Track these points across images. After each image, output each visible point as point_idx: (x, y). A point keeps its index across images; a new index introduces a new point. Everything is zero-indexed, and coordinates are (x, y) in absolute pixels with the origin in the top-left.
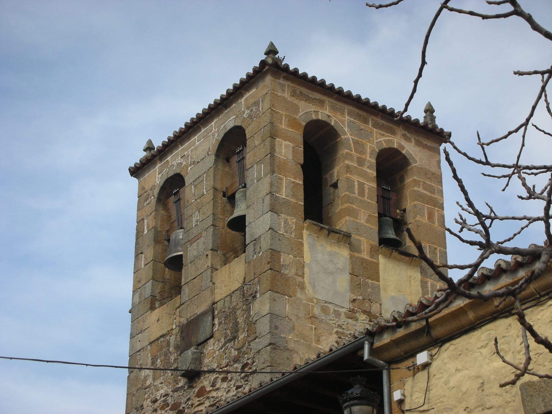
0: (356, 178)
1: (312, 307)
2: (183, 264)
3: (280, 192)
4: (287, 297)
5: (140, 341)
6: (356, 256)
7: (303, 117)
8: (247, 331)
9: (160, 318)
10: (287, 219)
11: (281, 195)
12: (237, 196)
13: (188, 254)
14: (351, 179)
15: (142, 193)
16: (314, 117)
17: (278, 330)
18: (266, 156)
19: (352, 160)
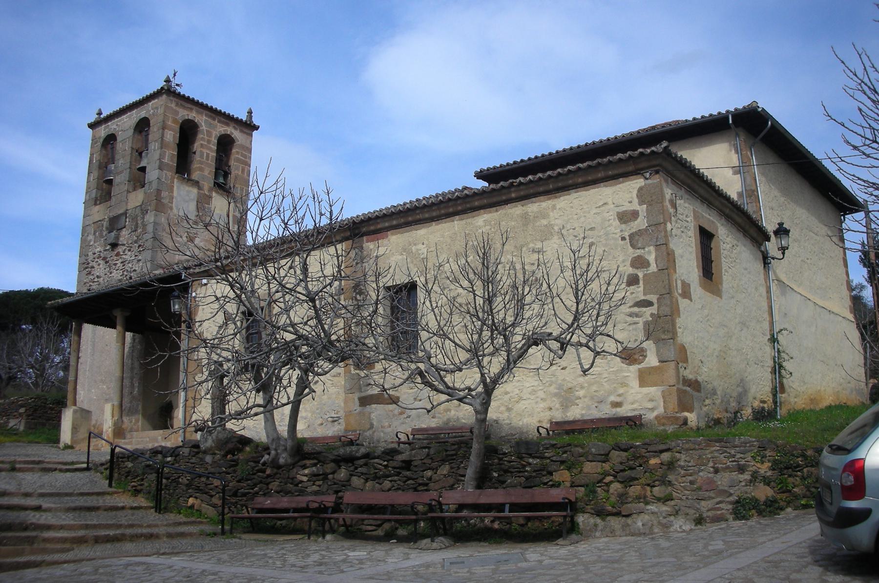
0: (205, 151)
12: (143, 154)
16: (187, 118)
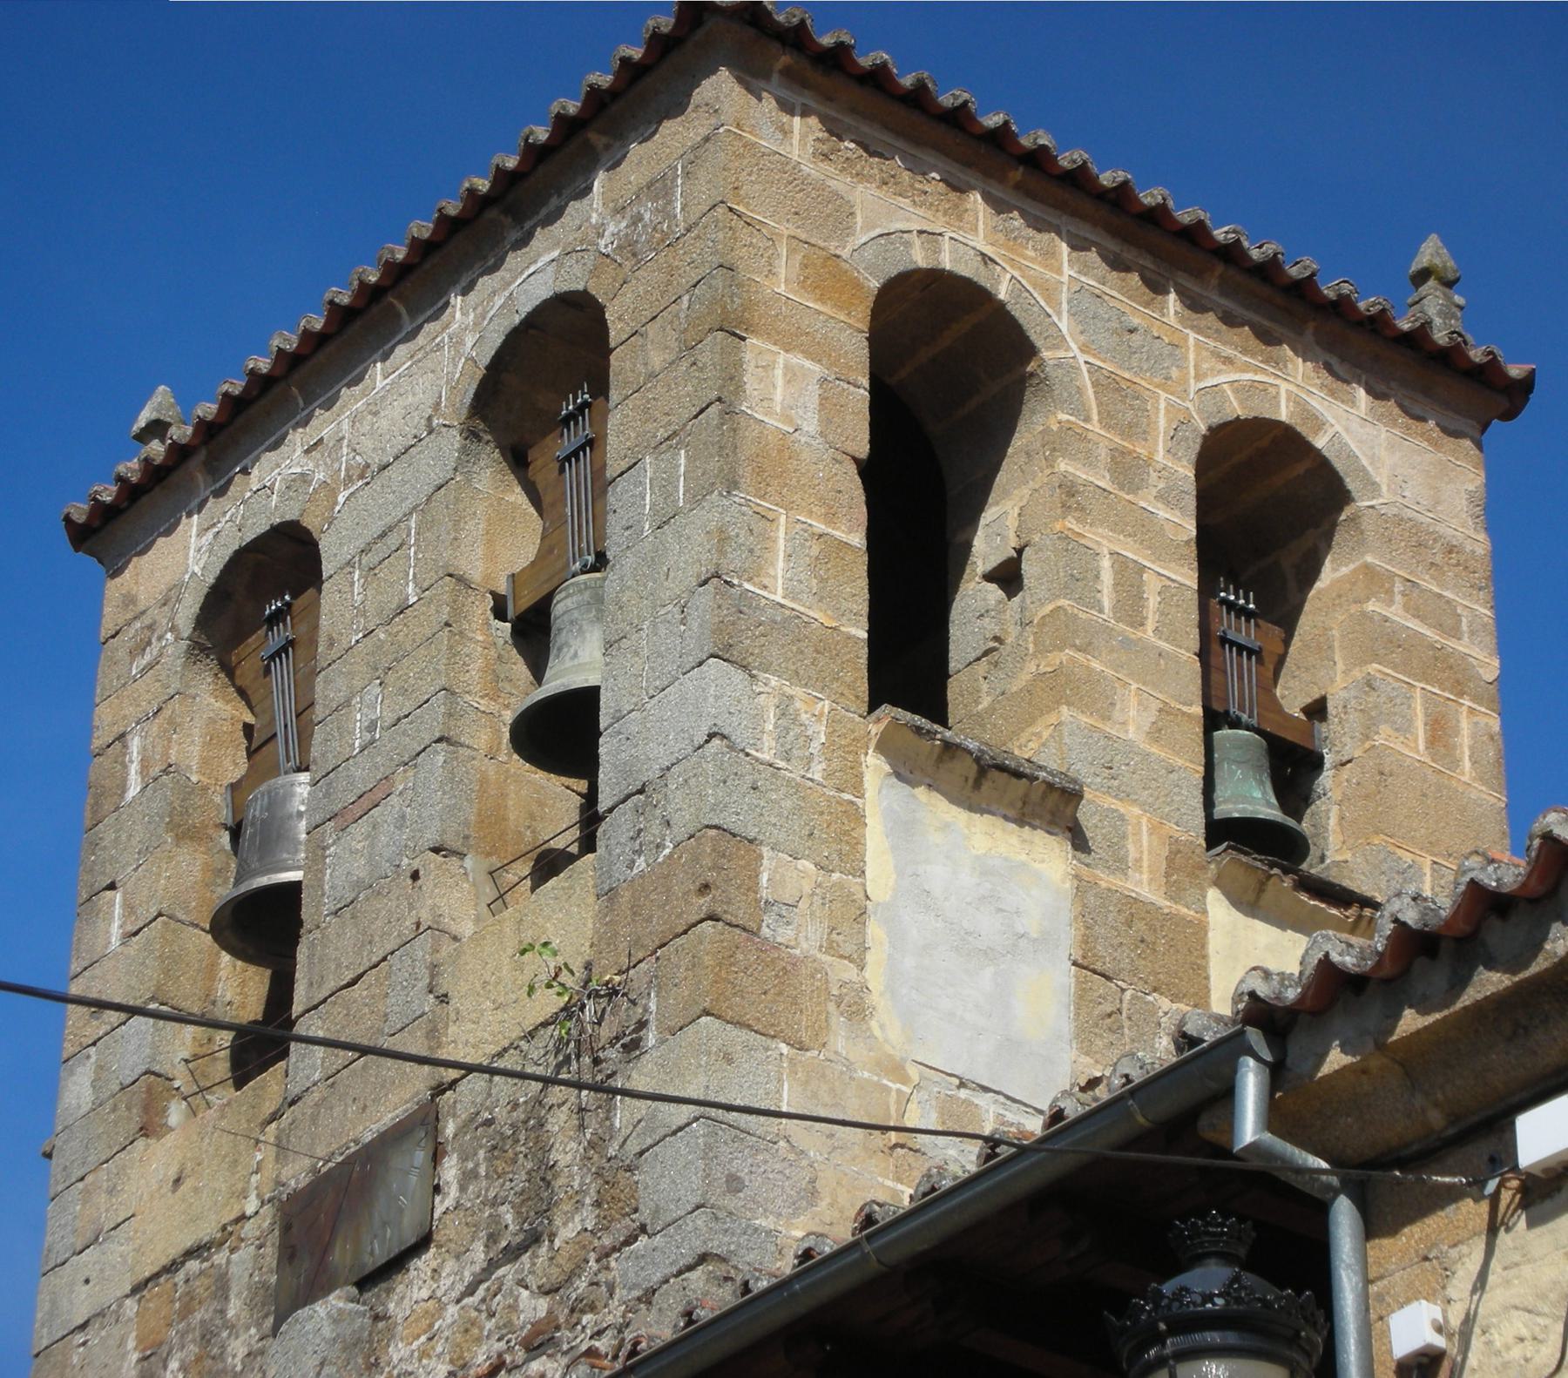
0: (1104, 542)
1: (898, 1102)
2: (300, 923)
3: (759, 576)
4: (784, 1048)
5: (87, 1281)
6: (1103, 884)
7: (868, 253)
8: (597, 1204)
9: (188, 1171)
10: (791, 698)
11: (765, 587)
12: (562, 606)
13: (327, 877)
14: (1083, 541)
15: (121, 622)
16: (920, 258)
17: (741, 1195)
18: (702, 411)
19: (1089, 460)
